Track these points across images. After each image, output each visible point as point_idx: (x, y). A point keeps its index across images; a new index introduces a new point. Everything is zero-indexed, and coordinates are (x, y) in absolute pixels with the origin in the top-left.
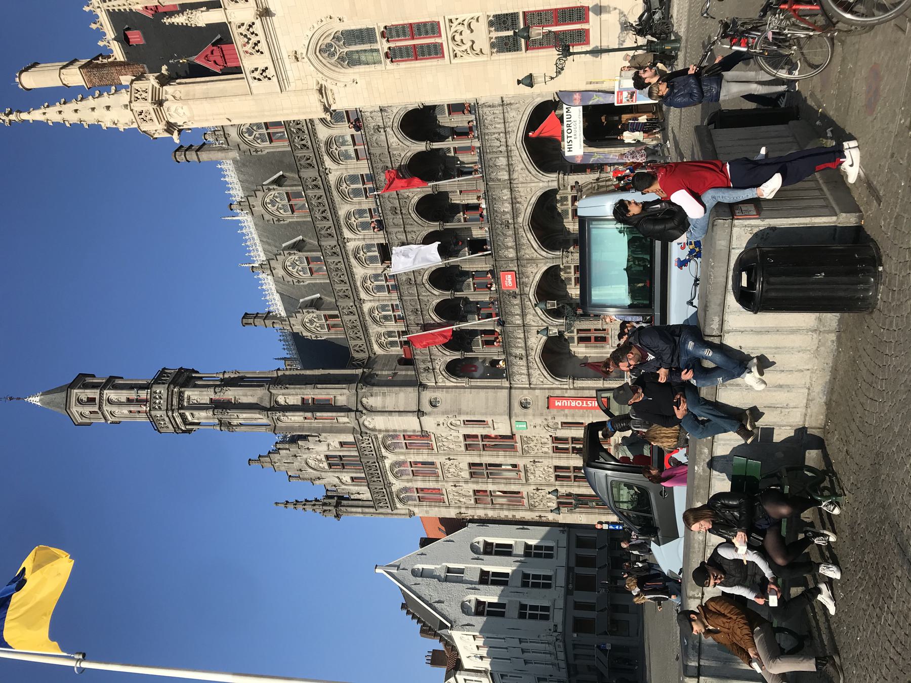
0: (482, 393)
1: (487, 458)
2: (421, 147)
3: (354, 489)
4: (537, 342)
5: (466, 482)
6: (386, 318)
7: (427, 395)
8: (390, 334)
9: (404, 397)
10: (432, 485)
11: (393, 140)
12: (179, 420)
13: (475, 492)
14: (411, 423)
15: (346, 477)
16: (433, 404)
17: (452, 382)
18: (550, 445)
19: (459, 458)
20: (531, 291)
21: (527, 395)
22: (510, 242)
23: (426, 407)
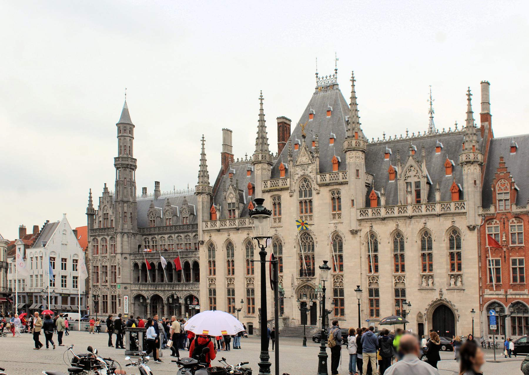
0: (129, 275)
1: (109, 273)
2: (191, 267)
3: (97, 221)
4: (144, 293)
5: (101, 264)
6: (153, 242)
7: (128, 256)
8: (149, 242)
9: (127, 249)
10: (99, 251)
11: (193, 259)
12: (118, 166)
13: (98, 267)
14: (119, 250)
15: (101, 219)
16: (126, 258)
17: (132, 264)
18: (114, 294)
19: (109, 263)
20: (157, 293)
21: (129, 289)
22: (169, 289)
23: (124, 256)
